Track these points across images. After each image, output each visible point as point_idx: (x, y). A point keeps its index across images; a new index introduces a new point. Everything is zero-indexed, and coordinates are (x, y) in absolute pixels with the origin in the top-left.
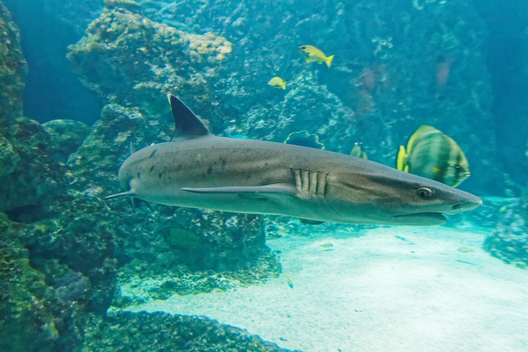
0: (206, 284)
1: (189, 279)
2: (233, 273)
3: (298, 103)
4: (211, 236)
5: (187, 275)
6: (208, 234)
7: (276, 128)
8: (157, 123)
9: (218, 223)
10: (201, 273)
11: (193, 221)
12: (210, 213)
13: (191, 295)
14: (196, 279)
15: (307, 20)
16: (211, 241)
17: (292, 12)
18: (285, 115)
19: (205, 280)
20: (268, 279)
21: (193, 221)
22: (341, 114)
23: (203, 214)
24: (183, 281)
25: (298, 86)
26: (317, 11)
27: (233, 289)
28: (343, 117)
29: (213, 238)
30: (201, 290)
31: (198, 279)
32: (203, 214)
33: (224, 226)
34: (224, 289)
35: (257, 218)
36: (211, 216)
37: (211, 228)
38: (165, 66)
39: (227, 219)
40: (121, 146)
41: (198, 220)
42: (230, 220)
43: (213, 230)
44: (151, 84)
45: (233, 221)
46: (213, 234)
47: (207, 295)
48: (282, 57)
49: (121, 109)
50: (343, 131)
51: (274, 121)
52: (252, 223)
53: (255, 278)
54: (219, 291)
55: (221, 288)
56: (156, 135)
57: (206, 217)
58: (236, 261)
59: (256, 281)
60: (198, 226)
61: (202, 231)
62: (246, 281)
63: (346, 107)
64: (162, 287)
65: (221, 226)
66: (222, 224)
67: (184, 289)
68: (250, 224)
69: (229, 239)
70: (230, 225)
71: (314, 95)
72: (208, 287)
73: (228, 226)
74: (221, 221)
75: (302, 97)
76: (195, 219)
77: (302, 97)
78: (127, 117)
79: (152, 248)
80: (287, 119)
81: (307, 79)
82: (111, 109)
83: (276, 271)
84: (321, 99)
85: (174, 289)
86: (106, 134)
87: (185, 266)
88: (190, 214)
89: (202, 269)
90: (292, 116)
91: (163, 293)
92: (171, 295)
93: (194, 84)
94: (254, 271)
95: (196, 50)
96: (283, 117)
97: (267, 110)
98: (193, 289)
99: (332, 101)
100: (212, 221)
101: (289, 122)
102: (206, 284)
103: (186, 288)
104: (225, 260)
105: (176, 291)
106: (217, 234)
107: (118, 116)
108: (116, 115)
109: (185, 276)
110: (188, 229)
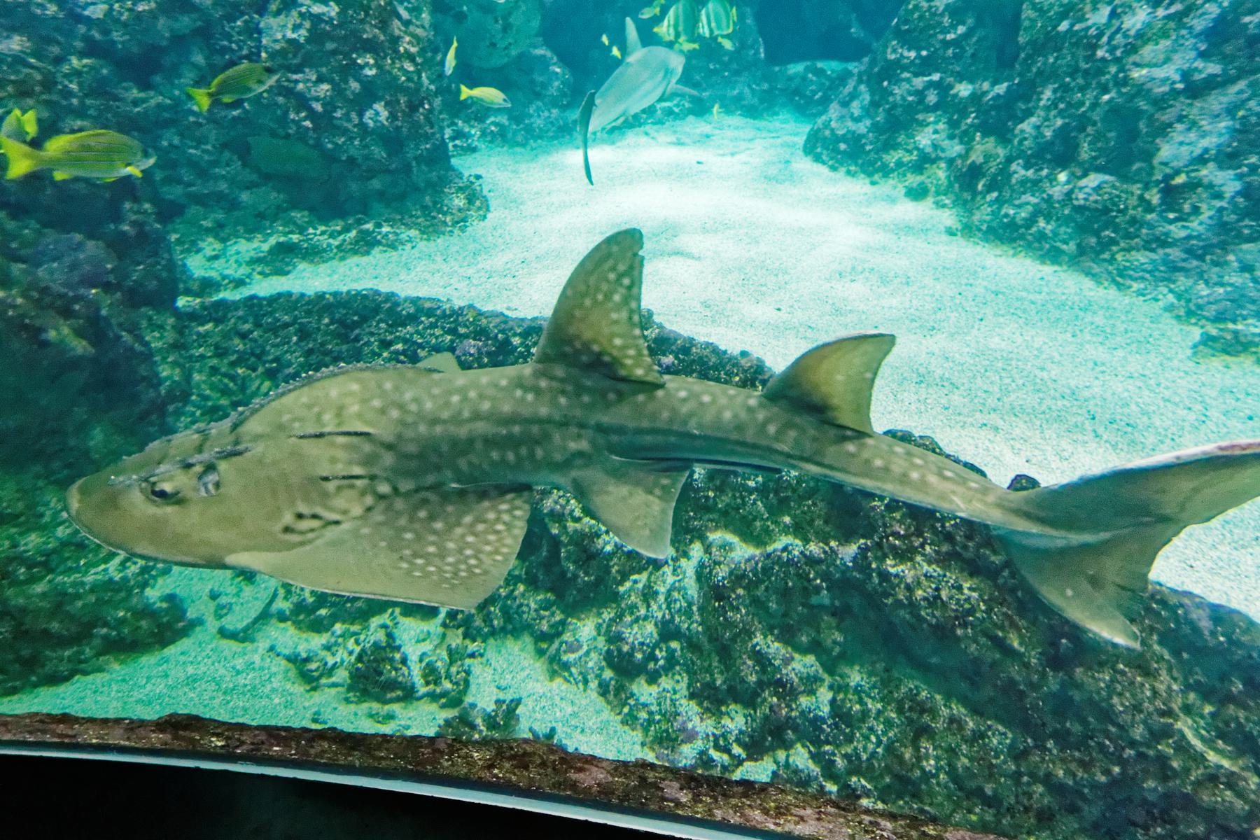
4: (340, 147)
5: (315, 229)
9: (349, 120)
10: (341, 223)
11: (292, 116)
13: (335, 263)
16: (344, 158)
19: (353, 233)
21: (292, 116)
23: (311, 99)
27: (409, 245)
31: (340, 233)
33: (362, 125)
34: (392, 246)
36: (329, 103)
41: (303, 114)
45: (377, 114)
47: (365, 259)
53: (445, 223)
55: (388, 246)
57: (318, 107)
60: (308, 128)
64: (271, 251)
65: (355, 126)
69: (379, 152)
73: (371, 124)
74: (354, 115)
83: (479, 209)
87: (306, 213)
91: (277, 264)
94: (440, 211)
102: (357, 242)
104: (381, 195)
109: (311, 231)
110: (288, 136)
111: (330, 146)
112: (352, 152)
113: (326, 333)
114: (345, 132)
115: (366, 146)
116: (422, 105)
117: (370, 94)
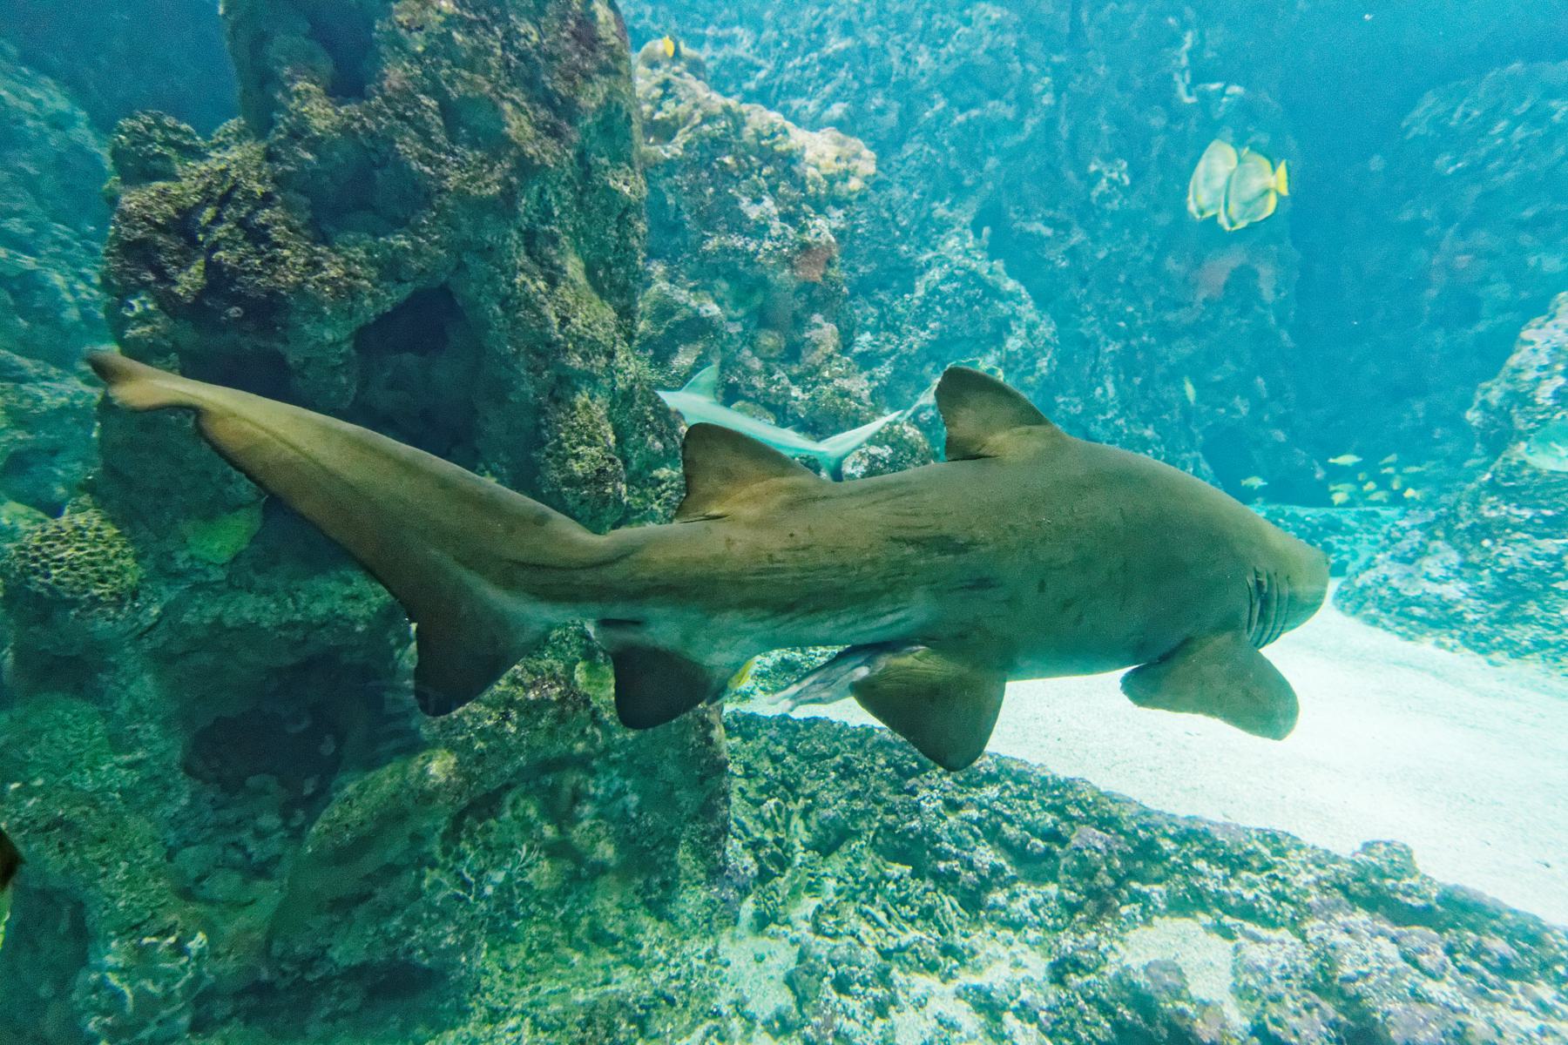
3: (946, 298)
15: (974, 113)
17: (946, 95)
25: (949, 262)
26: (995, 95)
28: (1036, 333)
38: (762, 200)
44: (737, 241)
48: (915, 196)
50: (1034, 361)
71: (981, 282)
75: (955, 285)
77: (955, 285)
80: (922, 334)
81: (967, 245)
84: (994, 292)
90: (932, 326)
93: (818, 243)
95: (817, 167)
113: (881, 776)
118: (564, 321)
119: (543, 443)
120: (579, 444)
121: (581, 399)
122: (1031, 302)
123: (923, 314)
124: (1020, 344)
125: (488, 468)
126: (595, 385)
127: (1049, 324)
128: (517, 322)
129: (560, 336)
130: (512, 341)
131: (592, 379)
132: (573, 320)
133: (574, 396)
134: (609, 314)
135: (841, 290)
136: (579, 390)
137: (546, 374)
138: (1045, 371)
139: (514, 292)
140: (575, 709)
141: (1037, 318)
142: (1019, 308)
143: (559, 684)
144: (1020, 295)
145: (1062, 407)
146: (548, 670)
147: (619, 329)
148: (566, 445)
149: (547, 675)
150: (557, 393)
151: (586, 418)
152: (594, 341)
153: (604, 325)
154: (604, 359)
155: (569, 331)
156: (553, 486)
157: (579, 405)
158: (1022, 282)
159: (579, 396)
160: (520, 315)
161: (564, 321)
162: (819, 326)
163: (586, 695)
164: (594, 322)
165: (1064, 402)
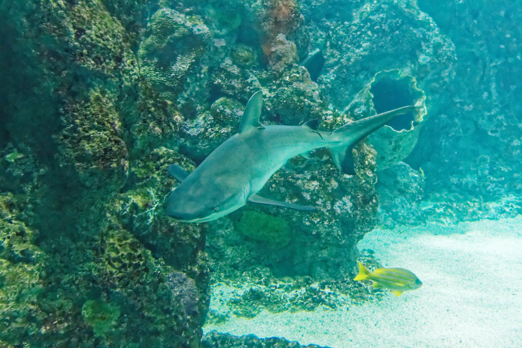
0: (307, 298)
1: (279, 288)
2: (337, 283)
3: (376, 24)
5: (275, 282)
6: (311, 222)
7: (341, 63)
8: (223, 43)
9: (325, 207)
12: (314, 190)
13: (287, 313)
14: (290, 289)
16: (314, 233)
18: (355, 44)
19: (303, 290)
20: (382, 293)
22: (437, 46)
23: (303, 191)
24: (273, 290)
27: (345, 306)
28: (440, 51)
29: (317, 228)
30: (300, 306)
31: (293, 288)
32: (303, 191)
33: (332, 211)
34: (333, 306)
35: (374, 201)
36: (316, 194)
37: (316, 214)
39: (337, 201)
40: (182, 77)
42: (341, 202)
43: (319, 216)
45: (345, 204)
46: (318, 223)
47: (310, 314)
49: (180, 18)
51: (337, 53)
52: (368, 208)
54: (327, 309)
56: (219, 63)
57: (307, 196)
58: (338, 265)
59: (370, 296)
61: (302, 217)
62: (358, 295)
63: (444, 36)
65: (328, 211)
66: (329, 208)
67: (275, 303)
68: (366, 209)
69: (337, 231)
70: (341, 210)
72: (310, 302)
73: (339, 211)
74: (328, 203)
75: (381, 15)
76: (291, 199)
77: (381, 15)
78: (191, 30)
79: (221, 239)
80: (357, 51)
82: (168, 16)
85: (262, 302)
86: (160, 57)
87: (268, 269)
88: (283, 189)
89: (293, 274)
90: (364, 45)
92: (259, 311)
96: (349, 46)
97: (324, 35)
98: (289, 303)
99: (424, 24)
100: (317, 202)
101: (360, 55)
102: (307, 298)
103: (278, 301)
104: (325, 261)
105: (266, 305)
106: (323, 223)
107: (177, 28)
108: (175, 26)
111: (308, 223)
112: (322, 230)
114: (321, 215)
115: (331, 226)
116: (371, 199)
117: (342, 191)
118: (80, 32)
119: (61, 127)
120: (91, 129)
121: (94, 94)
122: (437, 29)
123: (359, 36)
124: (429, 59)
125: (15, 146)
126: (106, 83)
127: (450, 45)
128: (40, 31)
129: (77, 43)
130: (37, 47)
131: (104, 78)
132: (88, 32)
133: (88, 91)
134: (119, 28)
135: (299, 16)
136: (93, 86)
137: (64, 73)
138: (447, 80)
139: (38, 8)
140: (80, 340)
141: (441, 41)
142: (428, 33)
143: (67, 320)
144: (429, 23)
145: (458, 105)
146: (60, 308)
147: (126, 40)
148: (80, 129)
149: (57, 313)
150: (73, 88)
151: (97, 108)
152: (105, 48)
153: (114, 36)
154: (113, 63)
155: (84, 39)
156: (68, 162)
157: (92, 98)
158: (431, 15)
159: (92, 91)
160: (43, 26)
161: (80, 32)
162: (282, 43)
163: (91, 328)
164: (106, 33)
165: (460, 102)
